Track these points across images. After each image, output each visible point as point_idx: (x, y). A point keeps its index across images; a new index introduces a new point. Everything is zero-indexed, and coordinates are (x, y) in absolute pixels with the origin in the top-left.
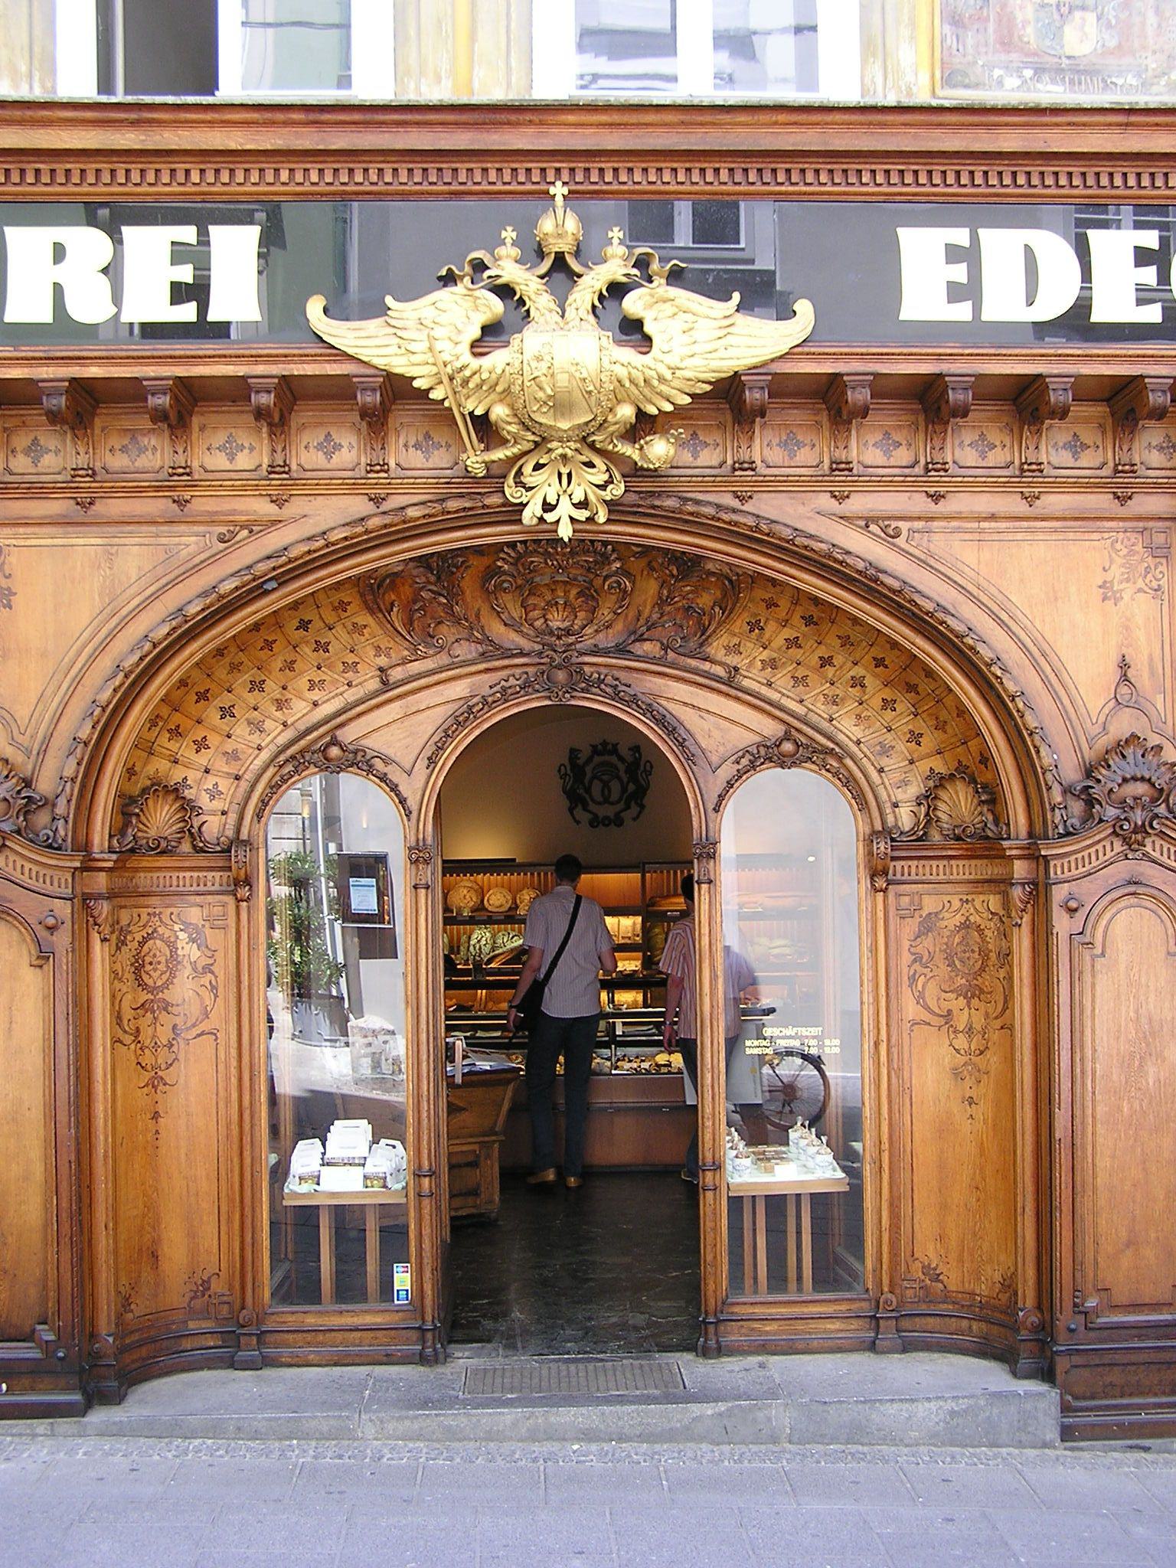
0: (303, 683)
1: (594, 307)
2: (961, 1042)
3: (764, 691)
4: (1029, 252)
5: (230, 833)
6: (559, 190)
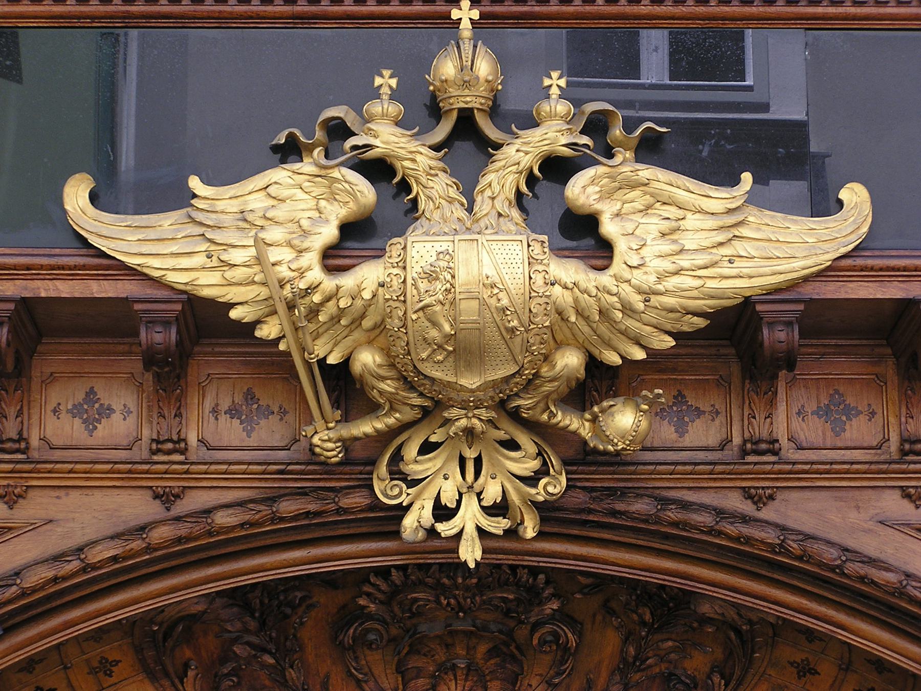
1: (519, 195)
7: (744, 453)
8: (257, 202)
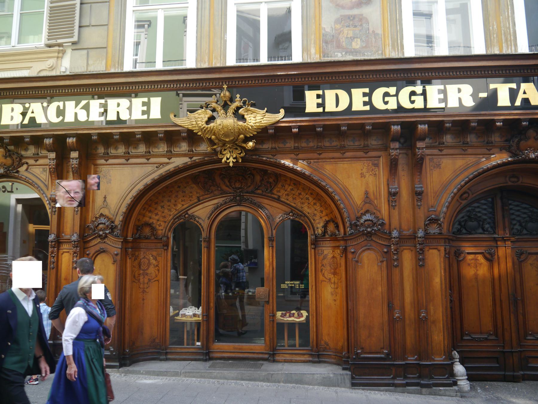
0: (180, 200)
2: (333, 286)
3: (286, 201)
4: (337, 96)
6: (225, 86)
8: (197, 115)
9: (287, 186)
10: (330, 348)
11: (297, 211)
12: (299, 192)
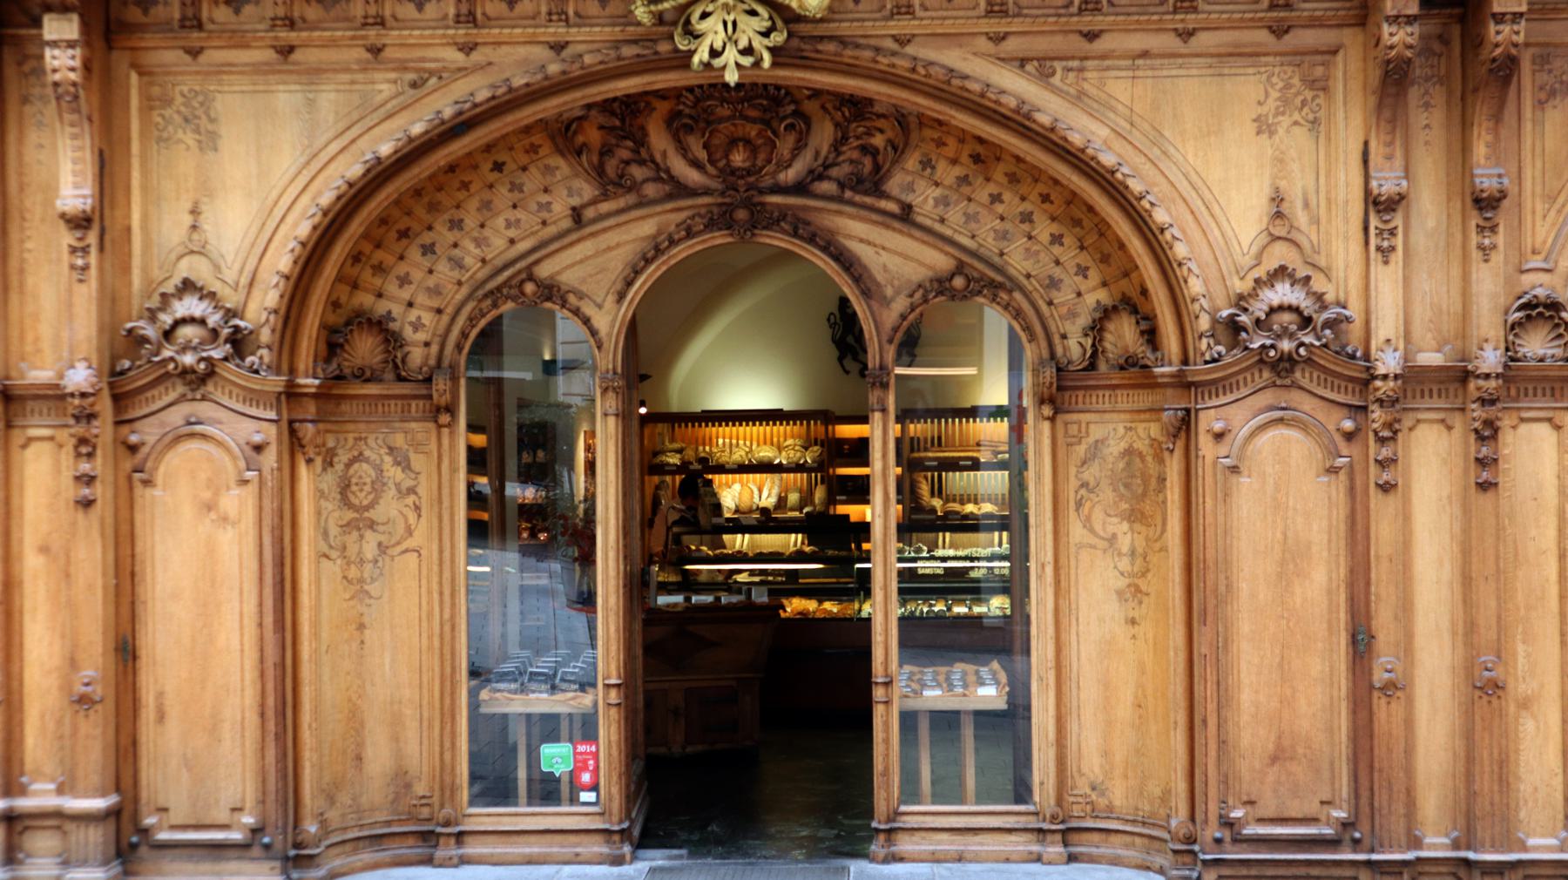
0: (500, 222)
3: (938, 227)
5: (432, 362)
7: (892, 14)
9: (942, 166)
10: (1110, 808)
11: (976, 264)
12: (992, 188)
